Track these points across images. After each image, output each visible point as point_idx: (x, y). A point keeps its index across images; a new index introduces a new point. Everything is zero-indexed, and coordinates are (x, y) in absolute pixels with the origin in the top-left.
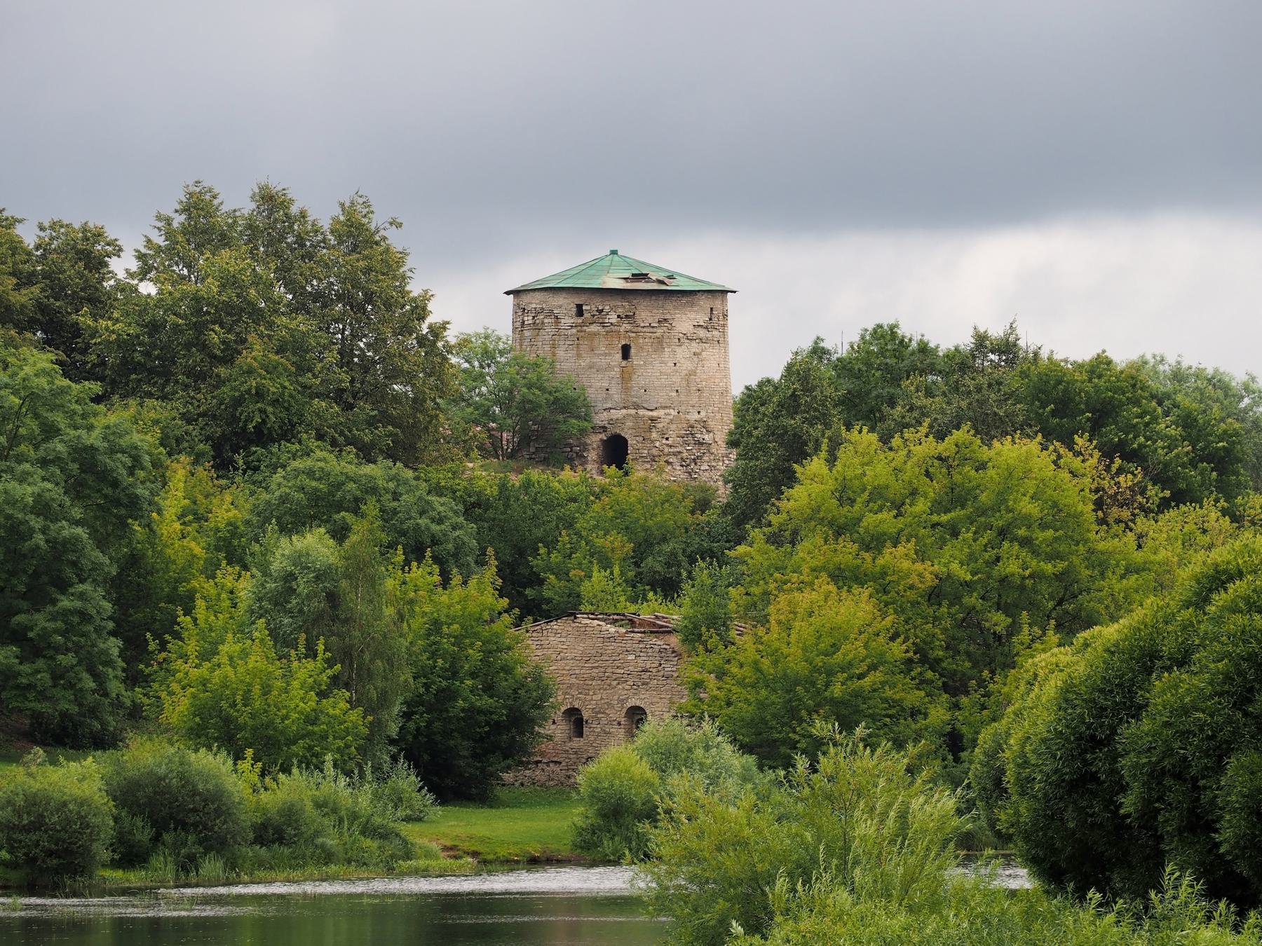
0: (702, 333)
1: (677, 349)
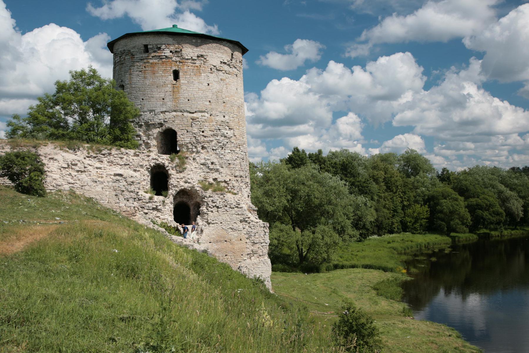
0: (226, 67)
1: (209, 74)
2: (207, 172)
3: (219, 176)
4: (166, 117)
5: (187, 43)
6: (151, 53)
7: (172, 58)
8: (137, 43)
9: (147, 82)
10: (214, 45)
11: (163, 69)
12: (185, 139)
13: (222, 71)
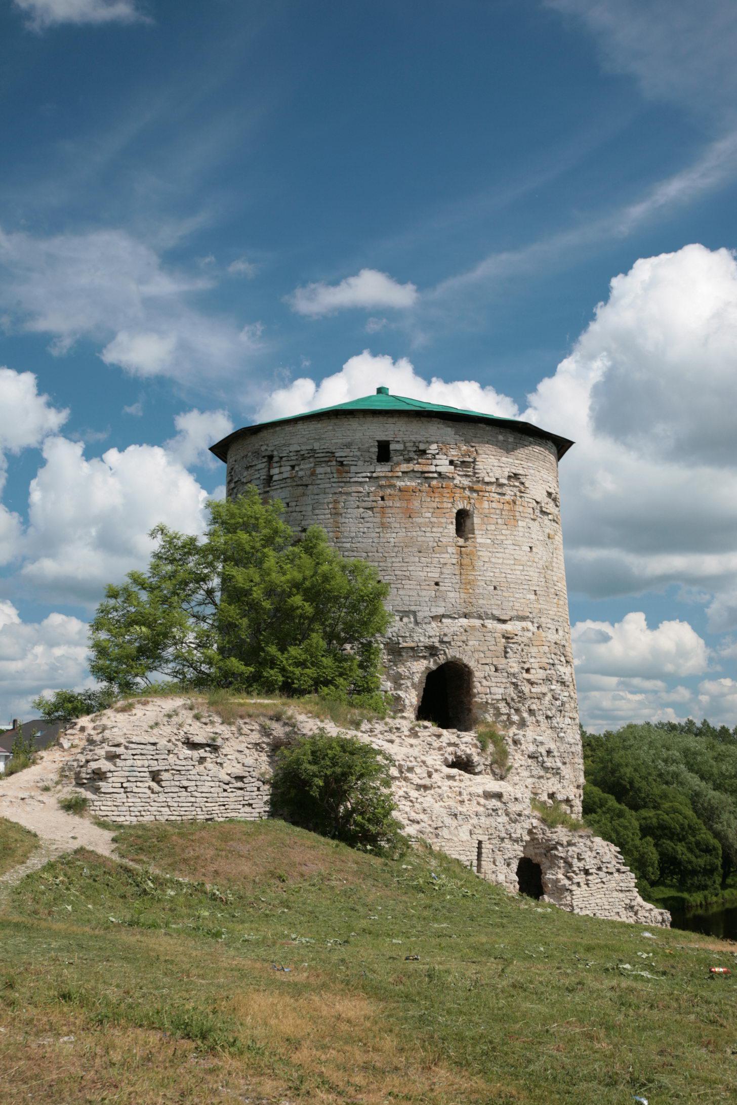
2: (540, 777)
3: (559, 786)
4: (446, 630)
5: (488, 443)
6: (398, 464)
7: (453, 478)
8: (358, 435)
9: (392, 537)
10: (537, 449)
11: (435, 505)
12: (494, 690)
13: (548, 514)
